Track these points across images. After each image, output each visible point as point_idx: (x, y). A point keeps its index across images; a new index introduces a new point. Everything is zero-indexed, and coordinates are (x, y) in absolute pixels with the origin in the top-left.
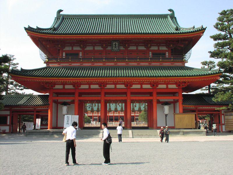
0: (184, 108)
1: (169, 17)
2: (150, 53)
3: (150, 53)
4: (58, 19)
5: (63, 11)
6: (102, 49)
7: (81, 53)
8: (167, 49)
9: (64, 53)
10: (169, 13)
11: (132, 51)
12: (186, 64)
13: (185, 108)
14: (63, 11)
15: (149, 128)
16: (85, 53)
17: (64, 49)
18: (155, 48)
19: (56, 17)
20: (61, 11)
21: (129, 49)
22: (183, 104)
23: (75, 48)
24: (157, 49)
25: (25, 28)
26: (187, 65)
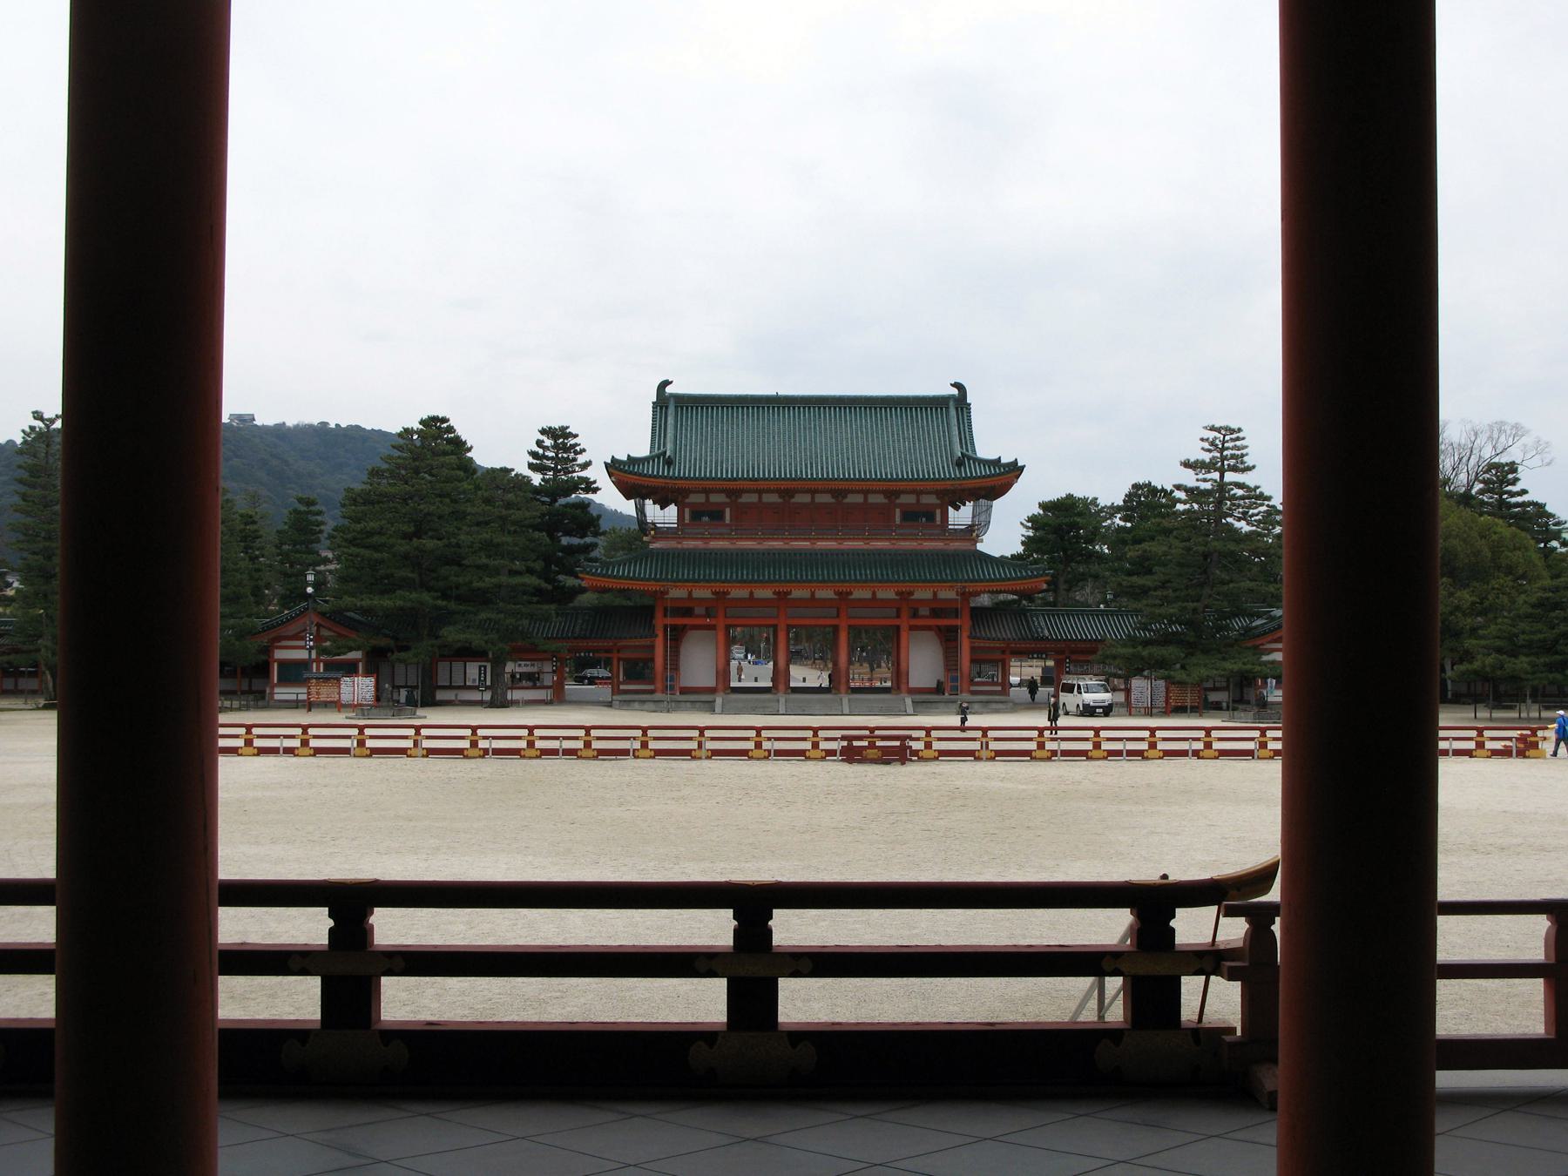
0: (973, 645)
1: (952, 404)
2: (898, 511)
3: (898, 511)
4: (661, 408)
5: (672, 382)
6: (780, 500)
7: (728, 511)
8: (938, 502)
9: (687, 511)
10: (955, 391)
11: (855, 506)
12: (978, 544)
13: (976, 644)
14: (672, 382)
15: (892, 690)
16: (741, 512)
17: (687, 501)
18: (910, 499)
19: (655, 400)
20: (665, 383)
21: (846, 501)
22: (969, 637)
23: (714, 498)
24: (914, 501)
25: (605, 463)
26: (980, 547)
